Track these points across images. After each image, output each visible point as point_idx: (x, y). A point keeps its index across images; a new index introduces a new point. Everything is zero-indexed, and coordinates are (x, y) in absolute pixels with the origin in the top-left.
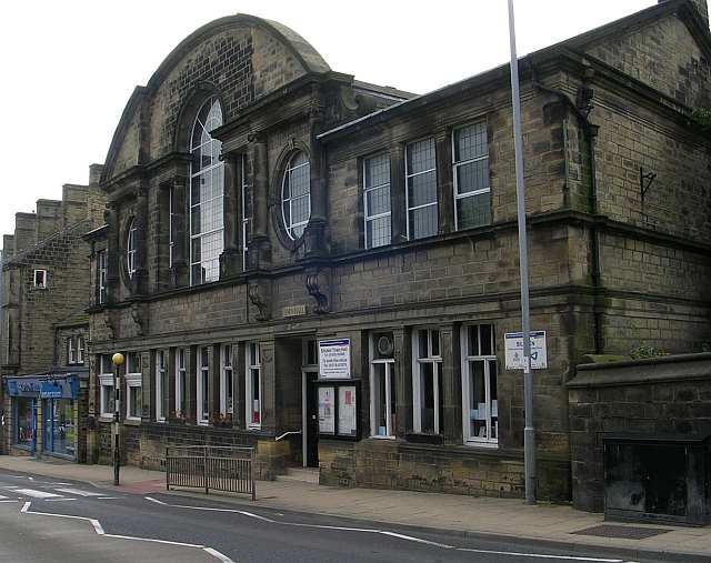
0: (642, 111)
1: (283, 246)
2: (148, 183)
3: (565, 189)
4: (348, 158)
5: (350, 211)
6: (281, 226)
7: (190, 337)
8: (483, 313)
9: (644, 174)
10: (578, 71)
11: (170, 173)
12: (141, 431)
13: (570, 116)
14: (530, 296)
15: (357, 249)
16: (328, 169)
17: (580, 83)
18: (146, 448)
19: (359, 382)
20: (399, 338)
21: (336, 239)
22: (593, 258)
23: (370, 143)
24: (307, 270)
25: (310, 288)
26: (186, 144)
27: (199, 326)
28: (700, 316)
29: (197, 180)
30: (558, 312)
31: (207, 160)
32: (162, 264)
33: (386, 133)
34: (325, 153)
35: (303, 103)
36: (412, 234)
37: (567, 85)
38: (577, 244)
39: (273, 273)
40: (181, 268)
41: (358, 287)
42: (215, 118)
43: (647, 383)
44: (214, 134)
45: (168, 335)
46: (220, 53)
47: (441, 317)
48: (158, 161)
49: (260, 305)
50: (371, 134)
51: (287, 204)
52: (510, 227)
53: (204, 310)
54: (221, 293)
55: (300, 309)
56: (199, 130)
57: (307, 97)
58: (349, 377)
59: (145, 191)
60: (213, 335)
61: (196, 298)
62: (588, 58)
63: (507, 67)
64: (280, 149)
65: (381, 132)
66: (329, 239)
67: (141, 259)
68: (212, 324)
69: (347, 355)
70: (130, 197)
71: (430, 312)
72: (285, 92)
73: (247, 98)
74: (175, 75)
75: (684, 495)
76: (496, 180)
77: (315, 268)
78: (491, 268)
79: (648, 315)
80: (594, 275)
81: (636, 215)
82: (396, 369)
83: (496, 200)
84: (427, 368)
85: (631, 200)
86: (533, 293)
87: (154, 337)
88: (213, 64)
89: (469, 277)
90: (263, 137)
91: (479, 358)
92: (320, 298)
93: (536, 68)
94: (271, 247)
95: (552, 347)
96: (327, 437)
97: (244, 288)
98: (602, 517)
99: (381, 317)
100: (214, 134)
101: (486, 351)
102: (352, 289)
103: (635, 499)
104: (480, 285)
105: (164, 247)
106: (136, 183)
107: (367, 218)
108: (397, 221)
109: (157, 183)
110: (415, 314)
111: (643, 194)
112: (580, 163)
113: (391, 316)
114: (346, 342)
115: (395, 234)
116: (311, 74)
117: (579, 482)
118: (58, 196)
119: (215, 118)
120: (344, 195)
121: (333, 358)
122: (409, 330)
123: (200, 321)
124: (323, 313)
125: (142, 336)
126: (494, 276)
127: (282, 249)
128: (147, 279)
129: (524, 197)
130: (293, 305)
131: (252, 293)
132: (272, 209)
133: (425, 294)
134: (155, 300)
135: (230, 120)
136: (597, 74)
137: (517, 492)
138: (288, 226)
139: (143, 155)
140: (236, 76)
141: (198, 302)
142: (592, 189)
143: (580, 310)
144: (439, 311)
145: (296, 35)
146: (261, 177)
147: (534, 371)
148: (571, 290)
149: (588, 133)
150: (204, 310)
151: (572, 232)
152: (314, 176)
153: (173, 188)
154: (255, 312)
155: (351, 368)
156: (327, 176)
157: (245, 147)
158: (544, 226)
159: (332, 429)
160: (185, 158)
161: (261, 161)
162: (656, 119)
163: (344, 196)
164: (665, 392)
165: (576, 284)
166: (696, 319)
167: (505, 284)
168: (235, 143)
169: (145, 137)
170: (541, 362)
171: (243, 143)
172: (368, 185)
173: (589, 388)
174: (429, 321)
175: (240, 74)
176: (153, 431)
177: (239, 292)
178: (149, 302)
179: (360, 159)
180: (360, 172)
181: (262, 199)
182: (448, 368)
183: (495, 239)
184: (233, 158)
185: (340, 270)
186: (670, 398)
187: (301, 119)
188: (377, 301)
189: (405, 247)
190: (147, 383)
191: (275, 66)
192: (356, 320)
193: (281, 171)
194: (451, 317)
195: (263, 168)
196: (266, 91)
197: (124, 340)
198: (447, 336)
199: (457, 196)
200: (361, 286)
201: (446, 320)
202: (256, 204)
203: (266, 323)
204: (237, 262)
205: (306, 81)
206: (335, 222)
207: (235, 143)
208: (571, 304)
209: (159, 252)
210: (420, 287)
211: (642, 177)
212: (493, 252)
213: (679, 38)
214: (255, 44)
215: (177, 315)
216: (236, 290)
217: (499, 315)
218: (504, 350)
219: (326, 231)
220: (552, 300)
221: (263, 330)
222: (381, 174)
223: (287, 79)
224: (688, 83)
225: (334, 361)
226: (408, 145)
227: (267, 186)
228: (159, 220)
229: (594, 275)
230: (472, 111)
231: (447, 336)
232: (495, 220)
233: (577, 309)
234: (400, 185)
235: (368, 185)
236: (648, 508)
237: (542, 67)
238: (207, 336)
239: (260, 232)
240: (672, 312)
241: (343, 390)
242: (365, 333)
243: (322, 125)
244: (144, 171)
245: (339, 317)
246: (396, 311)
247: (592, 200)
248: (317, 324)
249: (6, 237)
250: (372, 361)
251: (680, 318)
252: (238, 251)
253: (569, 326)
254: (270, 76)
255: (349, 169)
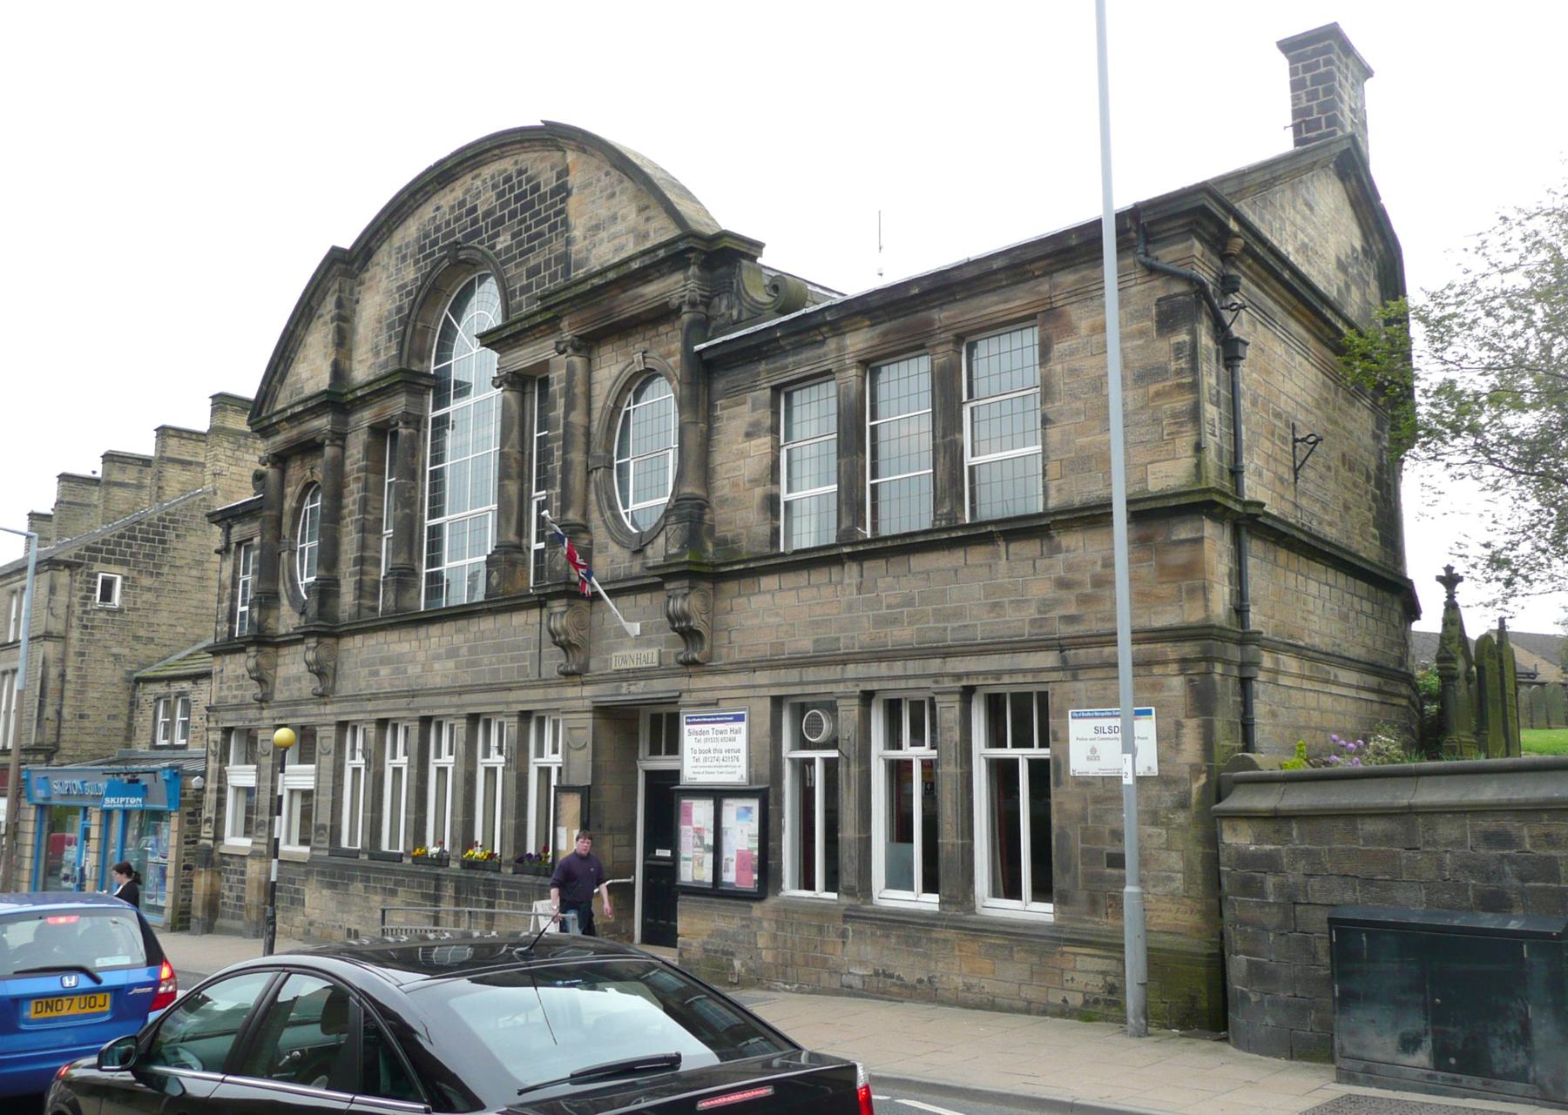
0: (1294, 326)
1: (618, 543)
2: (346, 424)
3: (1198, 448)
4: (752, 388)
5: (754, 482)
6: (612, 507)
7: (418, 701)
8: (1024, 671)
9: (1299, 436)
10: (1219, 241)
11: (398, 405)
12: (308, 873)
13: (1205, 318)
14: (1135, 642)
15: (767, 550)
16: (711, 407)
17: (1219, 263)
18: (317, 902)
19: (764, 794)
20: (849, 712)
21: (721, 531)
22: (1239, 577)
23: (797, 364)
24: (668, 586)
25: (672, 618)
26: (423, 356)
27: (437, 681)
28: (1358, 688)
29: (436, 421)
30: (1182, 672)
31: (463, 389)
32: (367, 568)
33: (832, 344)
34: (706, 378)
35: (675, 286)
36: (875, 526)
37: (1195, 258)
38: (1215, 543)
39: (723, 569)
40: (403, 577)
41: (768, 620)
42: (485, 309)
43: (1410, 812)
44: (489, 339)
45: (374, 697)
46: (500, 195)
47: (936, 677)
48: (369, 384)
49: (567, 647)
50: (799, 347)
51: (623, 470)
52: (1095, 516)
53: (452, 653)
54: (487, 624)
55: (649, 656)
56: (448, 334)
57: (678, 276)
58: (744, 781)
59: (340, 437)
60: (467, 698)
61: (434, 630)
62: (1240, 219)
63: (1097, 224)
64: (615, 370)
65: (823, 342)
66: (712, 529)
67: (328, 557)
68: (467, 679)
69: (741, 741)
70: (308, 448)
71: (913, 667)
72: (661, 253)
73: (553, 277)
74: (410, 230)
75: (1524, 1037)
76: (1054, 433)
77: (686, 583)
78: (1040, 589)
79: (1307, 685)
80: (1240, 610)
81: (1288, 508)
82: (842, 769)
83: (1054, 469)
84: (899, 771)
85: (1281, 480)
86: (1142, 636)
87: (346, 699)
88: (487, 214)
89: (995, 605)
90: (588, 344)
91: (1009, 752)
92: (690, 635)
93: (1146, 226)
94: (591, 543)
95: (1168, 739)
96: (696, 891)
97: (534, 615)
98: (1329, 1072)
99: (811, 674)
100: (489, 339)
101: (1022, 741)
102: (756, 622)
103: (1409, 1044)
104: (1018, 621)
105: (371, 538)
106: (323, 423)
107: (784, 496)
108: (851, 500)
109: (366, 424)
110: (882, 669)
111: (1296, 471)
112: (1218, 406)
113: (835, 672)
114: (739, 718)
115: (843, 526)
116: (689, 234)
117: (1254, 998)
118: (199, 419)
119: (485, 309)
120: (740, 455)
121: (712, 746)
122: (867, 697)
123: (442, 672)
124: (695, 663)
125: (322, 696)
126: (1046, 605)
127: (614, 548)
128: (337, 595)
129: (1133, 461)
130: (632, 640)
131: (556, 624)
132: (597, 475)
133: (902, 635)
134: (353, 633)
135: (514, 317)
136: (1247, 250)
137: (1101, 1008)
138: (626, 506)
139: (339, 373)
140: (531, 239)
141: (437, 637)
142: (1236, 455)
143: (1214, 665)
144: (935, 665)
145: (657, 168)
146: (577, 417)
147: (1140, 780)
148: (1201, 633)
149: (1230, 351)
150: (452, 653)
151: (1209, 529)
152: (688, 417)
153: (395, 435)
154: (554, 660)
155: (750, 765)
156: (710, 419)
157: (545, 364)
158: (1151, 514)
159: (706, 875)
160: (420, 381)
161: (579, 390)
162: (1312, 343)
163: (743, 455)
164: (1447, 830)
165: (1215, 621)
166: (1365, 695)
167: (1070, 619)
168: (524, 357)
169: (343, 340)
170: (1147, 759)
171: (541, 358)
172: (788, 437)
173: (1278, 818)
174: (912, 683)
175: (540, 235)
176: (338, 869)
177: (524, 623)
178: (338, 636)
179: (776, 389)
180: (776, 413)
181: (577, 456)
182: (948, 772)
183: (1051, 538)
184: (517, 382)
185: (731, 587)
186: (1461, 843)
187: (663, 314)
188: (805, 644)
189: (857, 548)
190: (328, 782)
191: (614, 218)
192: (762, 677)
193: (617, 408)
194: (958, 676)
195: (581, 403)
196: (595, 265)
197: (346, 699)
198: (949, 712)
199: (968, 460)
200: (767, 615)
201: (948, 683)
202: (566, 467)
203: (578, 679)
204: (519, 568)
205: (682, 246)
206: (723, 501)
207: (524, 357)
208: (1208, 659)
209: (363, 546)
210: (894, 621)
211: (1296, 441)
212: (1047, 561)
213: (1337, 209)
214: (574, 180)
215: (395, 661)
216: (518, 619)
217: (1055, 676)
218: (1067, 741)
219: (707, 517)
220: (1171, 650)
221: (571, 692)
222: (814, 416)
223: (636, 244)
224: (1348, 287)
225: (712, 752)
226: (870, 365)
227: (588, 433)
228: (365, 489)
229: (1240, 610)
230: (1019, 300)
231: (949, 712)
232: (1052, 503)
233: (1219, 668)
234: (854, 437)
235: (788, 437)
236: (1440, 1059)
237: (1156, 228)
238: (455, 700)
239: (573, 516)
240: (1336, 683)
241: (731, 808)
242: (777, 702)
243: (703, 327)
244: (338, 400)
245: (725, 672)
246: (844, 663)
247: (1236, 473)
248: (682, 683)
249: (759, 246)
250: (789, 753)
251: (1344, 691)
252: (520, 549)
253: (1202, 700)
254: (603, 234)
255: (754, 409)
